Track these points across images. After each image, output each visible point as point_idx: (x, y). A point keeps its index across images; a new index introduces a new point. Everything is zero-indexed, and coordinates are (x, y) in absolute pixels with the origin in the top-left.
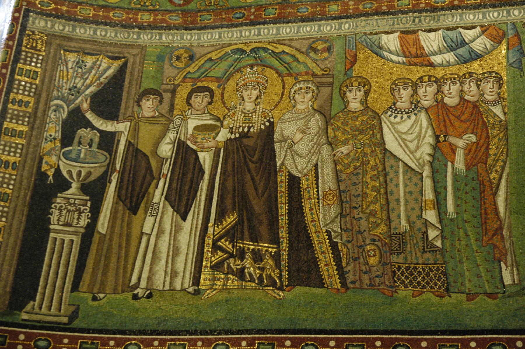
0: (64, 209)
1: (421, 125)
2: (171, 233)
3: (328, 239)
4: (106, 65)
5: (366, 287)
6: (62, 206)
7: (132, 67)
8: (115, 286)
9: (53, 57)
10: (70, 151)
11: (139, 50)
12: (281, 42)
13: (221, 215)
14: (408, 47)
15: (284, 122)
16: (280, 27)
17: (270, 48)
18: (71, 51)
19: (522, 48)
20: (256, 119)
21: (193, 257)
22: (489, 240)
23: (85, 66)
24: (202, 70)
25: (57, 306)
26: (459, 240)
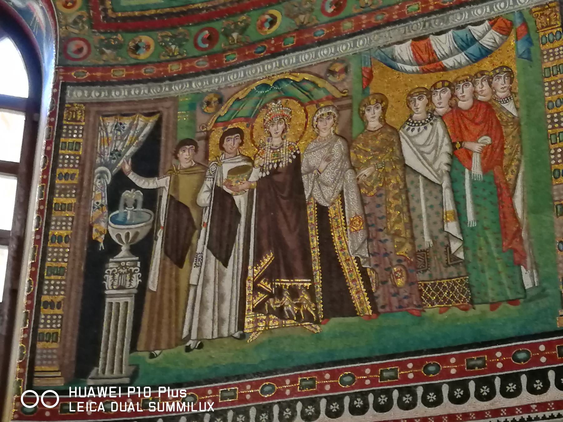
2: (215, 281)
3: (358, 266)
10: (118, 214)
12: (302, 70)
17: (291, 78)
20: (284, 153)
23: (124, 127)
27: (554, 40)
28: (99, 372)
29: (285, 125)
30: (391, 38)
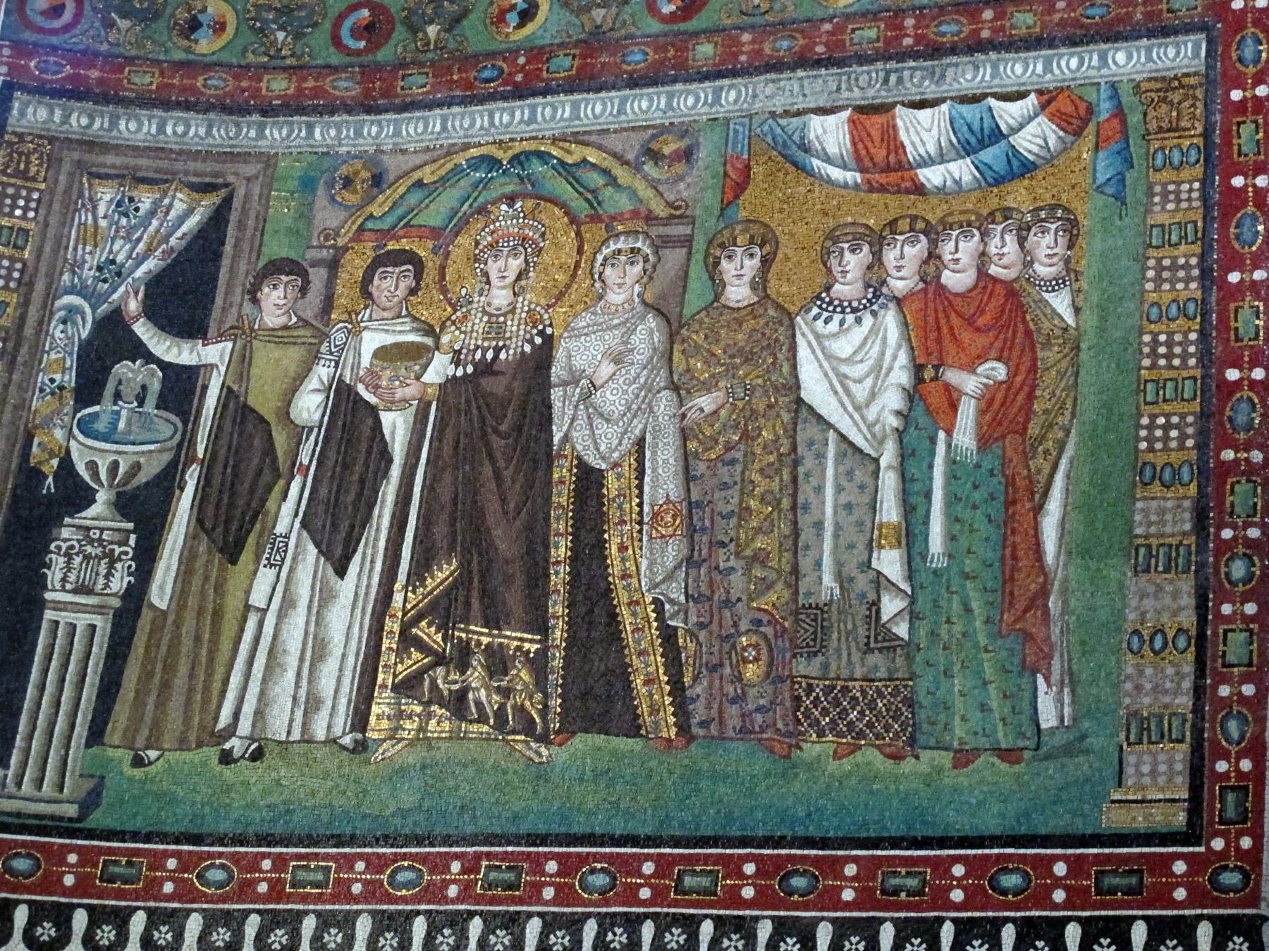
2: (310, 607)
3: (656, 620)
4: (185, 206)
5: (731, 733)
7: (243, 207)
9: (65, 192)
10: (96, 415)
11: (259, 166)
15: (576, 336)
16: (580, 101)
18: (107, 177)
20: (515, 328)
22: (1015, 622)
23: (137, 209)
24: (400, 211)
26: (948, 621)
27: (1182, 162)
28: (8, 781)
29: (526, 261)
30: (804, 95)
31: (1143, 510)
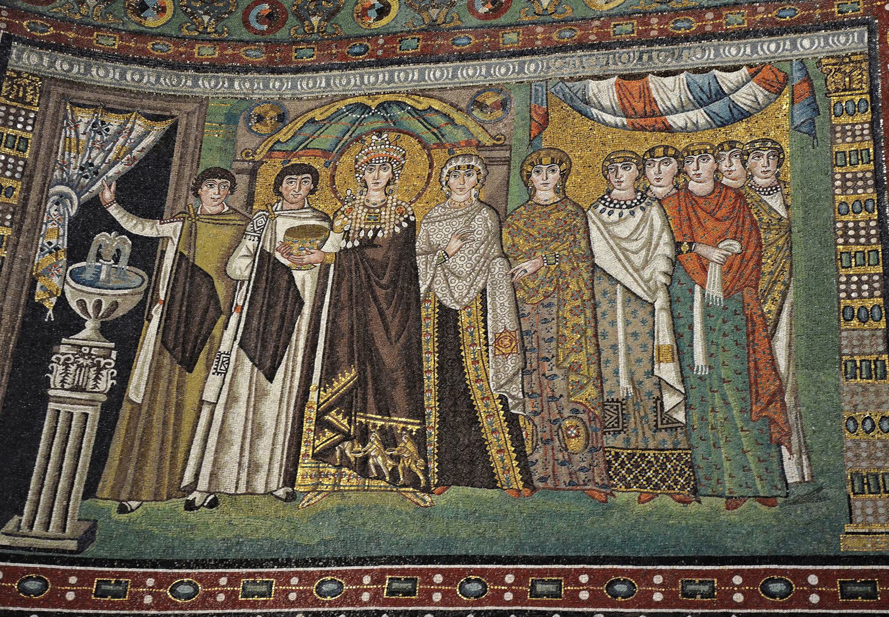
0: (72, 364)
1: (652, 226)
6: (69, 359)
8: (156, 489)
10: (84, 268)
11: (195, 105)
13: (329, 374)
14: (631, 100)
18: (84, 106)
19: (815, 101)
20: (387, 217)
21: (285, 439)
22: (761, 411)
23: (108, 130)
24: (299, 139)
25: (59, 523)
26: (713, 410)
29: (393, 173)
31: (847, 337)
